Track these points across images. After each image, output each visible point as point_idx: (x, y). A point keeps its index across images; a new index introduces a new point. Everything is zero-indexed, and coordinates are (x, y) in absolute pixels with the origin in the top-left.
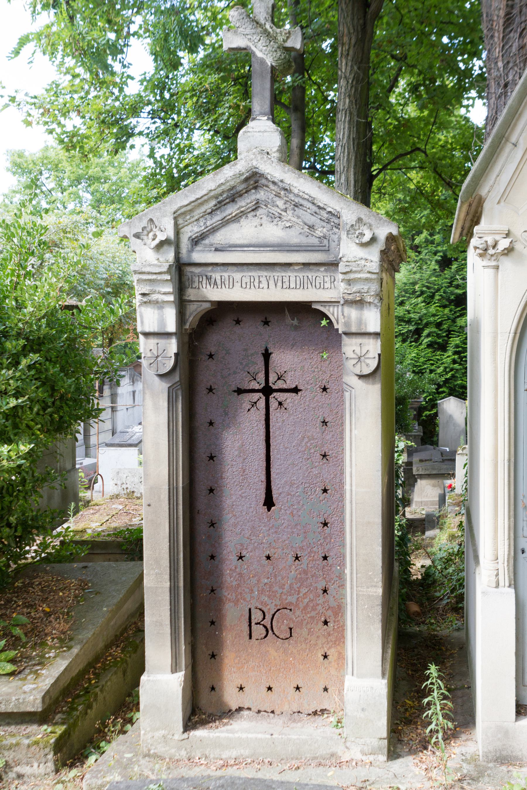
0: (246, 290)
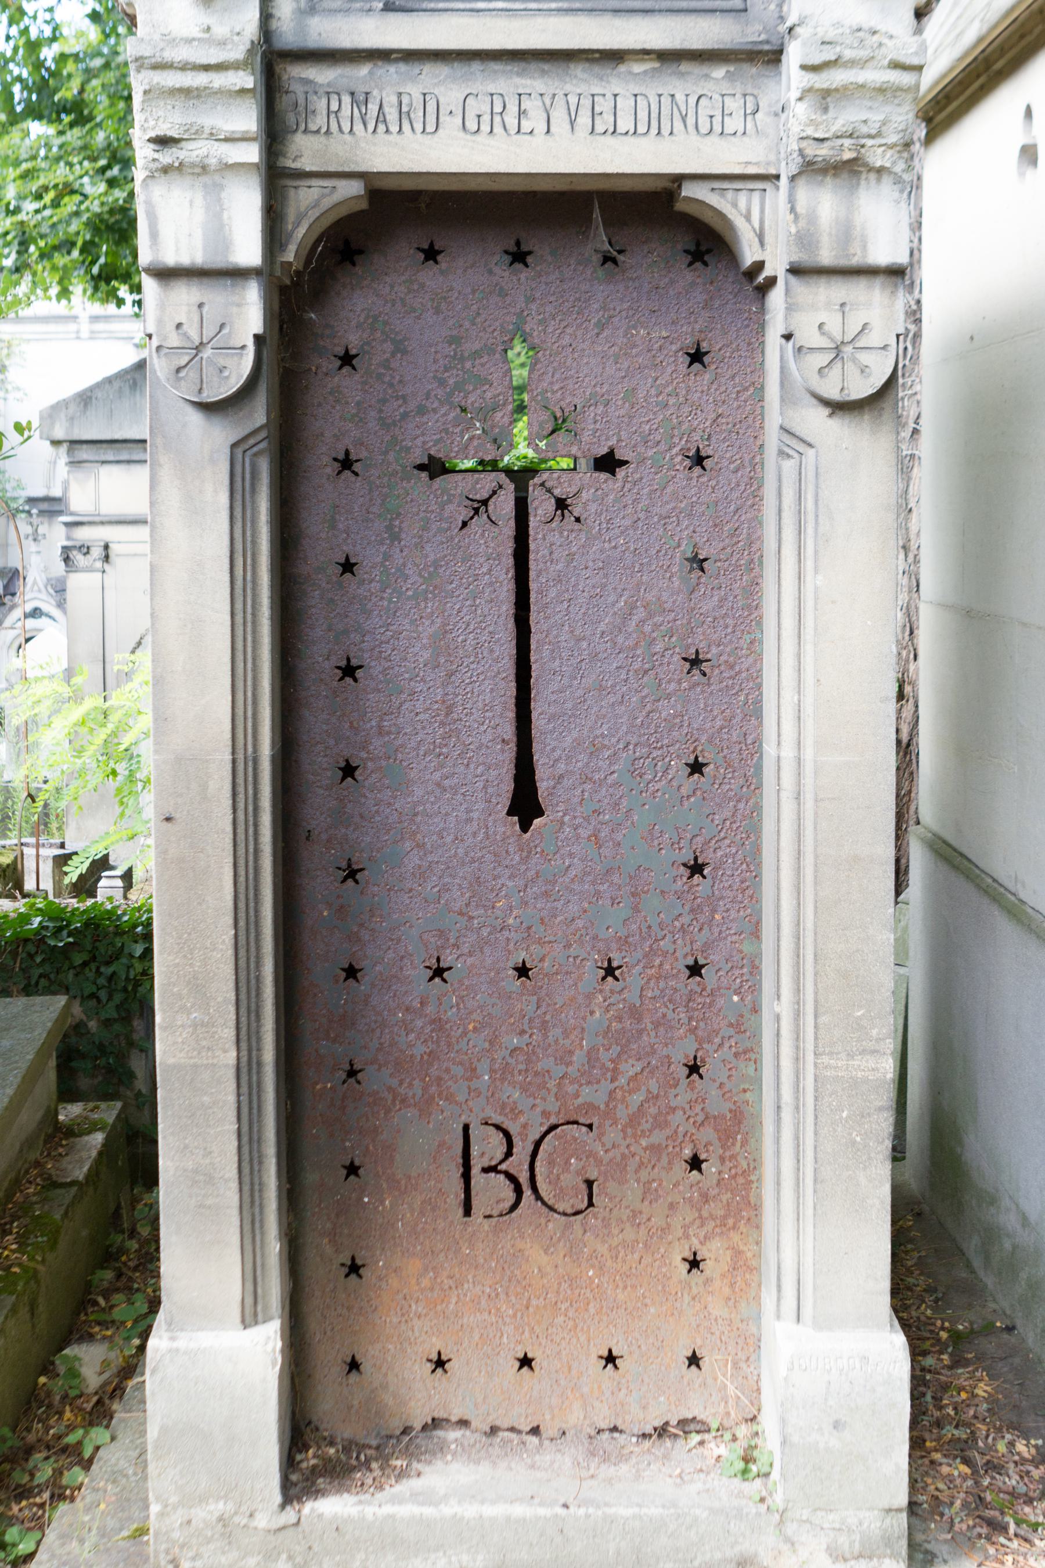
0: (480, 138)
